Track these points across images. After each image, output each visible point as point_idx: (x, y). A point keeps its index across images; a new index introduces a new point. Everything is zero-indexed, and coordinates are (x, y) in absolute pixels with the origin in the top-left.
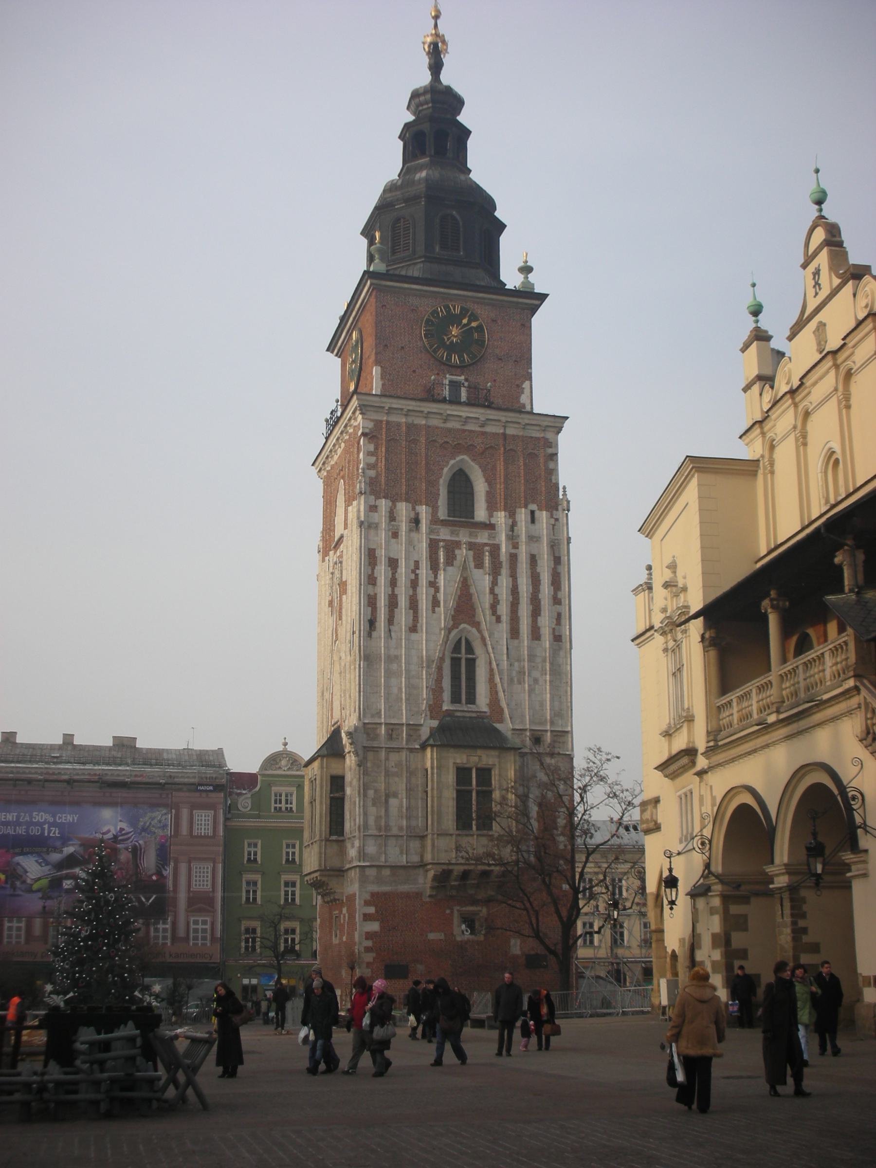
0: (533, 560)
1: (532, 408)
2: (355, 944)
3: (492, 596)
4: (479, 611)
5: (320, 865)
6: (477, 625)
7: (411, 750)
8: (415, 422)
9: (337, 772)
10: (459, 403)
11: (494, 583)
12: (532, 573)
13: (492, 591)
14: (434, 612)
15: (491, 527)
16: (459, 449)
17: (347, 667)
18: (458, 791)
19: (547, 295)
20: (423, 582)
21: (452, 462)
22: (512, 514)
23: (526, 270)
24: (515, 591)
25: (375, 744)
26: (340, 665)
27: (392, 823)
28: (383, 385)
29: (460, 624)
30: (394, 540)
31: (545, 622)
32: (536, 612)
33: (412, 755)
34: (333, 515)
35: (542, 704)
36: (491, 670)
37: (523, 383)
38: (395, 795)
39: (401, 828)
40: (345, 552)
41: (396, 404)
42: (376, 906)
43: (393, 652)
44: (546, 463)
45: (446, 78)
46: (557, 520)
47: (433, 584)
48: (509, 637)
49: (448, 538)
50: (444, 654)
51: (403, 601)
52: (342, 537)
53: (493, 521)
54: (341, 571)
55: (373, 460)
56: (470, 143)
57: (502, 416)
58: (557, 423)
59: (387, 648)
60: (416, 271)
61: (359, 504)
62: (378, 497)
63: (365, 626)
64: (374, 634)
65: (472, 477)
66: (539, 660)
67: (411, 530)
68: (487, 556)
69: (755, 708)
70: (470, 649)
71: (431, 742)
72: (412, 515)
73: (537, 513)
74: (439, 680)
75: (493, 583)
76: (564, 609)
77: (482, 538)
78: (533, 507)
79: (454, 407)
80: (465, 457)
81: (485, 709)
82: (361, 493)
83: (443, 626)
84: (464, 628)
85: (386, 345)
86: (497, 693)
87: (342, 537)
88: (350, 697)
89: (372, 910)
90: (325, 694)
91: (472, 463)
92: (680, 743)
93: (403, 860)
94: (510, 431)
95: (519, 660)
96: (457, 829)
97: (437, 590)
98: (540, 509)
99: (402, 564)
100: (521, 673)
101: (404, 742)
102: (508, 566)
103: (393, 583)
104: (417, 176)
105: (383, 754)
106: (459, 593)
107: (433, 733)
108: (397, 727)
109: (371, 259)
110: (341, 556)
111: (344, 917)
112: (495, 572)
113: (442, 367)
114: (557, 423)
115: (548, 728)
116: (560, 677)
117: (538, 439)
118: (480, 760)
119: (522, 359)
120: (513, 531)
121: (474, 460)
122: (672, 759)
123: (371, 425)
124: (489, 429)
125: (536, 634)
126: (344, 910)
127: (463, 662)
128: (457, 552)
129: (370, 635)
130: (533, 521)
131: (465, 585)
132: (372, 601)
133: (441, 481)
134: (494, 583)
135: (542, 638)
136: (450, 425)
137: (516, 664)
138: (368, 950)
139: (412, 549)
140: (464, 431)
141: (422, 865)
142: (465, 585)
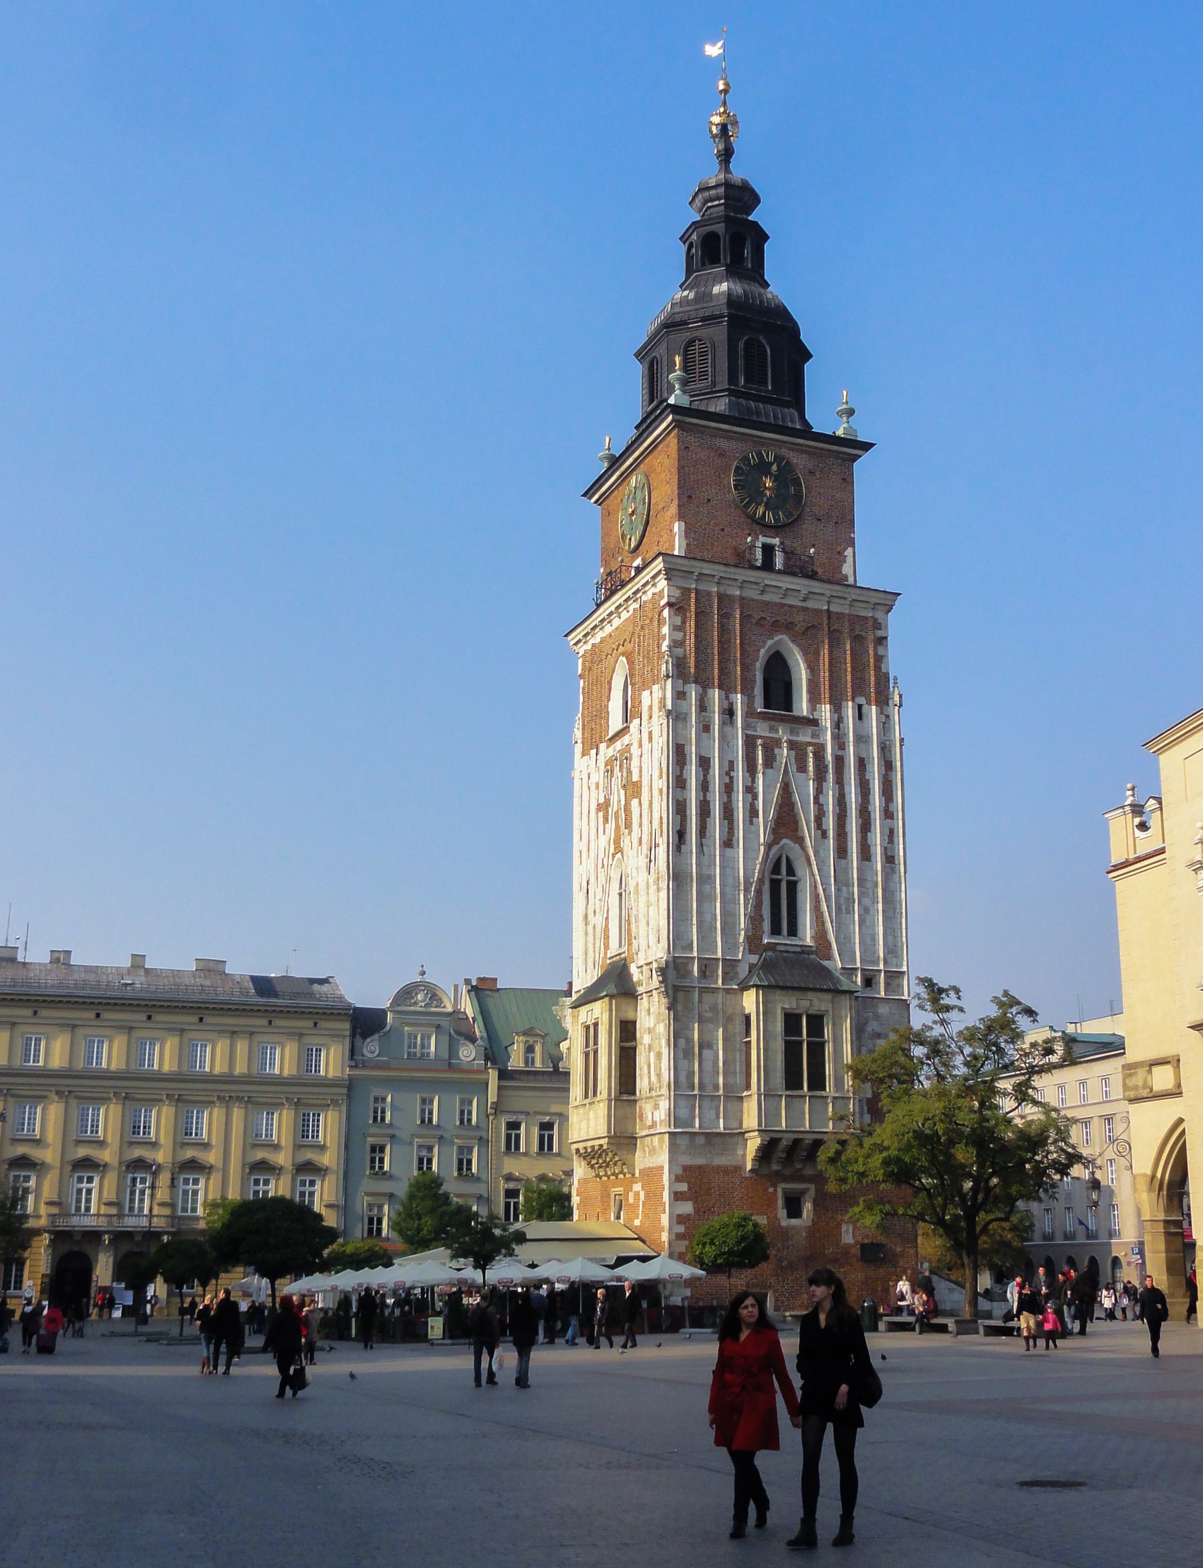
0: (862, 764)
1: (855, 581)
2: (662, 1229)
5: (609, 1131)
6: (800, 841)
7: (728, 991)
8: (728, 593)
9: (630, 1016)
11: (819, 791)
13: (816, 798)
15: (814, 722)
16: (776, 627)
18: (787, 1042)
19: (873, 445)
21: (770, 642)
24: (841, 801)
27: (706, 1080)
30: (704, 735)
32: (865, 827)
33: (729, 996)
35: (874, 939)
36: (817, 896)
41: (707, 569)
42: (689, 1183)
43: (705, 872)
46: (887, 717)
47: (750, 790)
55: (679, 636)
57: (826, 589)
58: (887, 600)
60: (721, 405)
61: (664, 689)
65: (790, 662)
66: (869, 885)
70: (791, 871)
72: (726, 706)
73: (865, 709)
74: (758, 906)
77: (804, 737)
78: (861, 700)
79: (773, 576)
80: (784, 637)
82: (668, 676)
85: (690, 497)
86: (823, 923)
89: (683, 1187)
90: (591, 916)
96: (787, 1088)
97: (755, 797)
101: (720, 982)
103: (704, 786)
104: (716, 290)
105: (696, 995)
111: (637, 1194)
112: (820, 777)
114: (887, 600)
117: (866, 618)
118: (811, 1005)
119: (844, 519)
124: (810, 604)
126: (637, 1187)
127: (784, 886)
130: (860, 717)
131: (786, 790)
132: (680, 808)
134: (819, 791)
135: (873, 859)
136: (766, 598)
138: (680, 1237)
140: (784, 605)
142: (786, 790)
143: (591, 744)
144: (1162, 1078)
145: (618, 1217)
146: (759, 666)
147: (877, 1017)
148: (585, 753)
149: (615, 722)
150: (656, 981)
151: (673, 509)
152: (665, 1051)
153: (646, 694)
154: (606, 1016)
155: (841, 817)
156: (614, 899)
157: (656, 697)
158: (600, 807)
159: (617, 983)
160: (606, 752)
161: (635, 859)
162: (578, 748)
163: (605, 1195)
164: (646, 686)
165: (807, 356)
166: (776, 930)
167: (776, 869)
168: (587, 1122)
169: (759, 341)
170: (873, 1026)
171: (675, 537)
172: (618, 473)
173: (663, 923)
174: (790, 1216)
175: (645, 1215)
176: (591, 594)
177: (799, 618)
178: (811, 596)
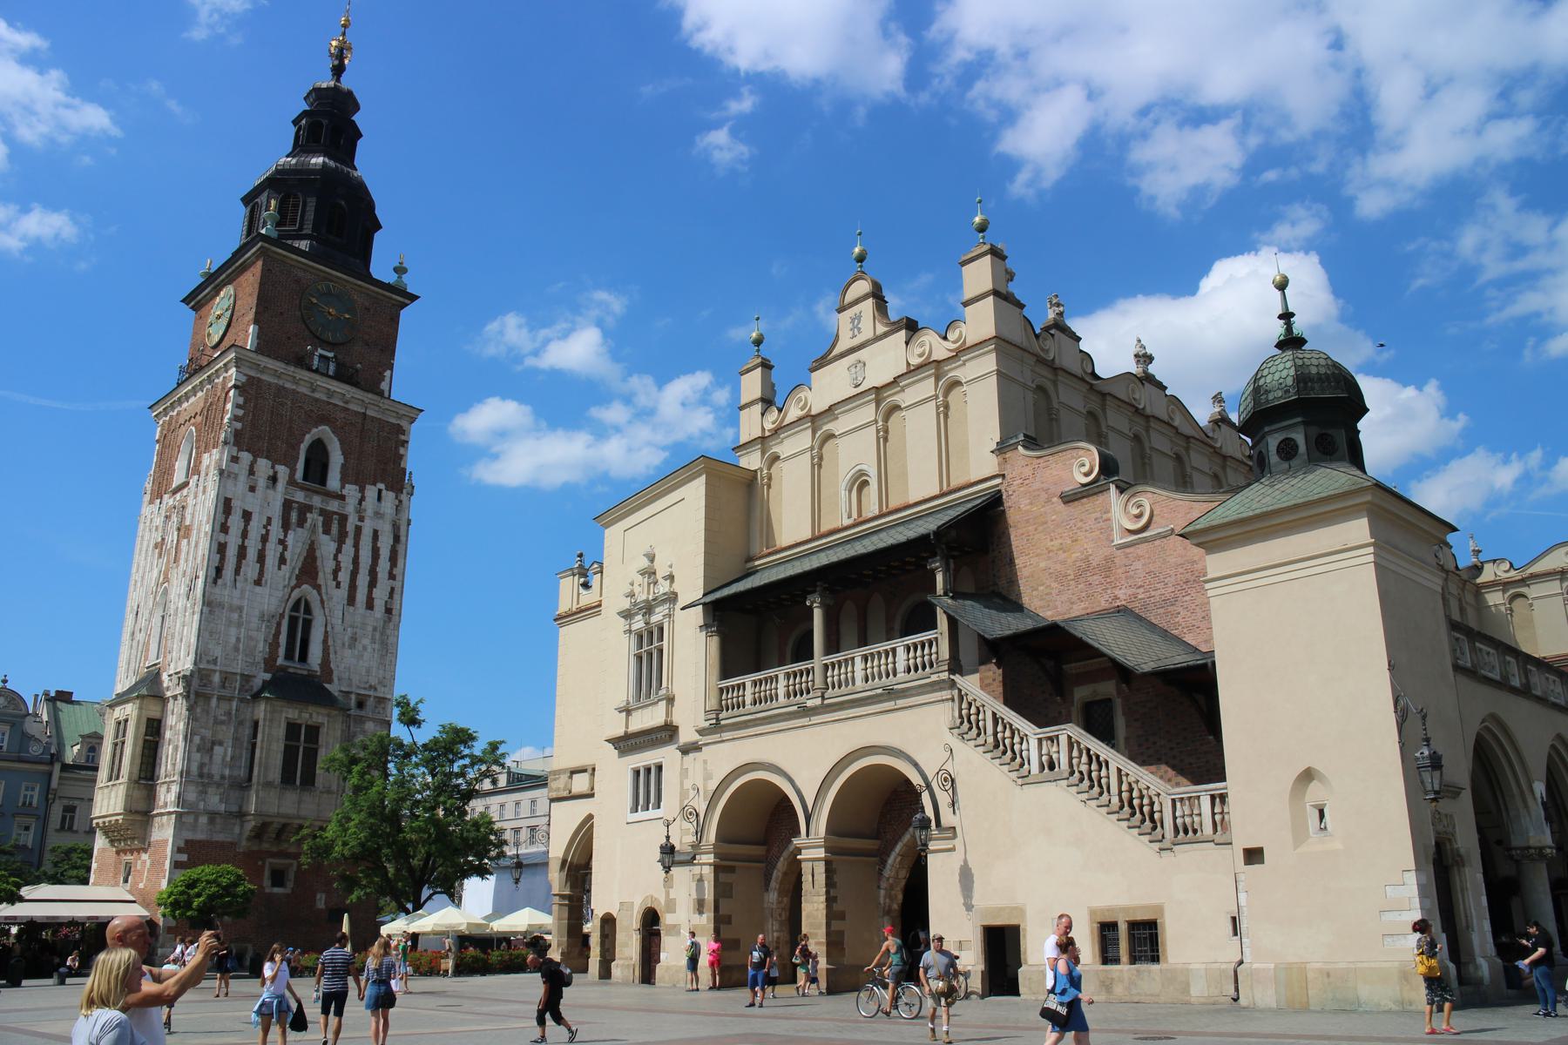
4: (321, 575)
6: (318, 588)
9: (155, 714)
10: (327, 376)
11: (339, 550)
13: (336, 557)
15: (343, 498)
16: (323, 420)
22: (362, 490)
23: (400, 270)
25: (208, 691)
31: (380, 594)
32: (373, 584)
38: (221, 744)
39: (223, 777)
43: (236, 602)
44: (397, 448)
45: (346, 82)
47: (282, 542)
51: (252, 554)
53: (345, 492)
55: (240, 413)
56: (360, 143)
58: (413, 413)
62: (240, 450)
63: (213, 573)
65: (329, 448)
68: (335, 524)
69: (781, 691)
70: (308, 610)
76: (397, 584)
78: (382, 486)
82: (225, 443)
89: (184, 857)
92: (650, 718)
93: (222, 808)
97: (285, 548)
99: (255, 517)
100: (354, 639)
103: (245, 535)
104: (313, 161)
105: (214, 702)
107: (266, 685)
112: (341, 541)
114: (413, 413)
115: (371, 693)
116: (387, 648)
119: (387, 348)
122: (627, 737)
123: (244, 379)
124: (352, 407)
129: (215, 582)
130: (379, 499)
132: (221, 548)
134: (339, 550)
136: (317, 395)
141: (241, 815)
143: (158, 494)
144: (580, 784)
145: (126, 881)
146: (304, 447)
147: (364, 732)
148: (151, 502)
149: (178, 478)
150: (180, 690)
151: (251, 315)
152: (181, 744)
153: (206, 456)
154: (135, 713)
155: (354, 574)
156: (157, 620)
157: (212, 459)
158: (156, 546)
159: (149, 688)
160: (168, 500)
161: (178, 588)
162: (147, 498)
163: (118, 863)
164: (207, 450)
165: (379, 227)
166: (289, 655)
167: (296, 607)
168: (109, 801)
170: (359, 738)
171: (249, 336)
173: (193, 640)
174: (274, 885)
175: (149, 880)
176: (174, 378)
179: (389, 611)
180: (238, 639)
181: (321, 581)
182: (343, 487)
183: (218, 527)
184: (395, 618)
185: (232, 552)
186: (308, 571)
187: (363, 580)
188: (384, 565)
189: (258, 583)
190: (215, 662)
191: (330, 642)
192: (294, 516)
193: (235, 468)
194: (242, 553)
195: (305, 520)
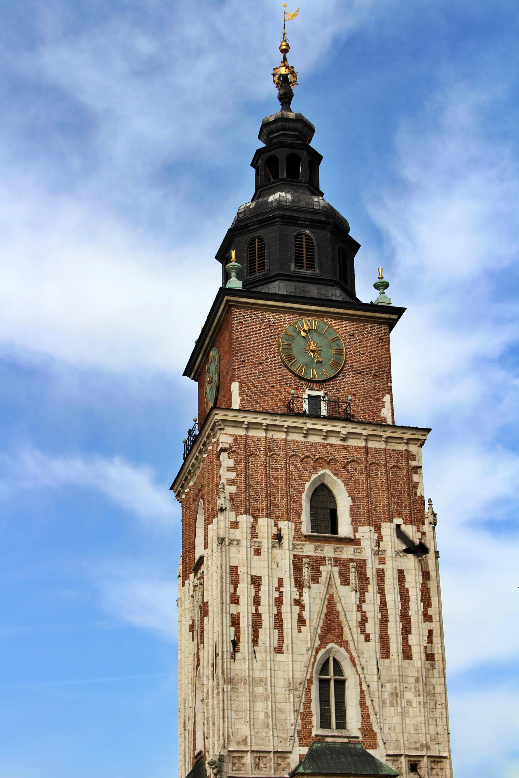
0: (401, 575)
1: (393, 422)
3: (359, 614)
4: (346, 629)
6: (345, 644)
11: (362, 600)
12: (400, 589)
13: (359, 608)
14: (300, 631)
17: (210, 692)
20: (287, 600)
22: (378, 529)
24: (383, 608)
26: (203, 691)
28: (242, 400)
29: (327, 644)
32: (406, 630)
34: (192, 536)
37: (383, 397)
40: (205, 574)
41: (255, 419)
43: (257, 674)
44: (409, 477)
46: (424, 534)
47: (298, 602)
48: (379, 655)
49: (312, 554)
50: (311, 677)
51: (267, 620)
52: (202, 558)
53: (358, 536)
54: (203, 592)
55: (232, 475)
59: (251, 669)
63: (230, 647)
64: (238, 656)
65: (335, 492)
67: (273, 547)
68: (354, 572)
71: (301, 770)
72: (275, 531)
75: (360, 599)
76: (434, 626)
77: (348, 552)
78: (398, 521)
79: (313, 422)
80: (328, 471)
81: (358, 734)
83: (309, 645)
84: (332, 648)
86: (368, 716)
87: (202, 558)
88: (214, 724)
91: (335, 478)
94: (372, 444)
95: (389, 681)
97: (302, 608)
98: (405, 523)
99: (265, 581)
100: (395, 694)
101: (273, 772)
102: (375, 582)
103: (257, 601)
104: (271, 198)
106: (325, 611)
108: (264, 755)
109: (226, 276)
110: (202, 577)
112: (362, 588)
113: (301, 382)
115: (424, 753)
117: (401, 452)
120: (379, 546)
121: (336, 474)
123: (230, 440)
125: (407, 654)
128: (322, 568)
129: (233, 657)
133: (304, 496)
134: (362, 600)
137: (388, 685)
139: (275, 566)
140: (325, 445)
169: (307, 235)
172: (202, 352)
177: (339, 455)
178: (349, 436)
179: (430, 657)
180: (267, 713)
181: (347, 636)
182: (356, 531)
183: (227, 598)
184: (438, 664)
185: (245, 623)
186: (332, 627)
187: (394, 628)
188: (416, 607)
189: (279, 650)
190: (245, 741)
191: (368, 703)
192: (306, 572)
193: (236, 534)
194: (257, 622)
195: (319, 574)
